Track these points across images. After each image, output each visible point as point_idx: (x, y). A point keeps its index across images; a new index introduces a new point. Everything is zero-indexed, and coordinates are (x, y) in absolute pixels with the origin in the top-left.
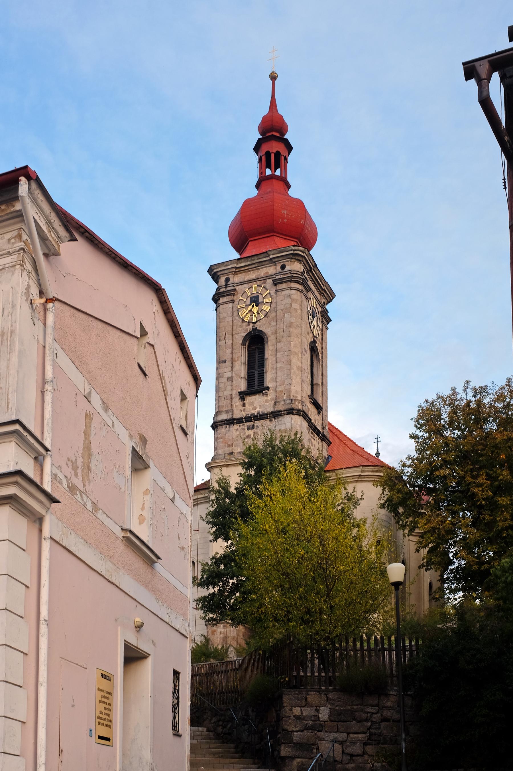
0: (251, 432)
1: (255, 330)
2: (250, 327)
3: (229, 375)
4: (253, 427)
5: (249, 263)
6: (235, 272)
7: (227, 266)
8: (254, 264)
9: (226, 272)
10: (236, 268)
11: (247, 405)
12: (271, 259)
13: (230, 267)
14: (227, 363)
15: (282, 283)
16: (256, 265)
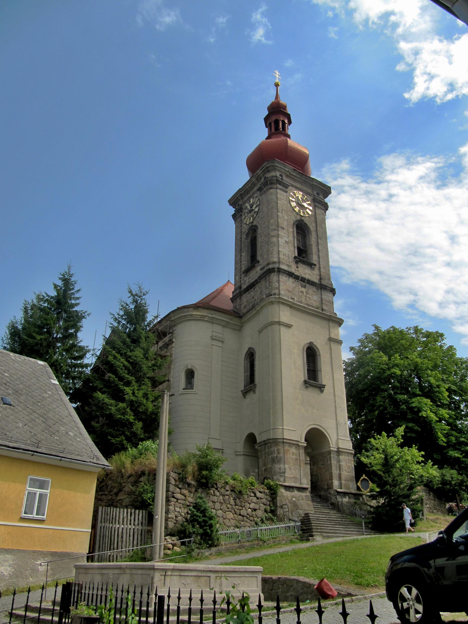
0: (303, 290)
1: (301, 220)
2: (299, 218)
3: (287, 240)
4: (305, 287)
5: (298, 176)
6: (287, 175)
7: (285, 167)
8: (301, 179)
9: (282, 170)
10: (290, 174)
11: (300, 269)
12: (313, 185)
13: (287, 169)
14: (285, 231)
15: (319, 203)
16: (302, 181)
